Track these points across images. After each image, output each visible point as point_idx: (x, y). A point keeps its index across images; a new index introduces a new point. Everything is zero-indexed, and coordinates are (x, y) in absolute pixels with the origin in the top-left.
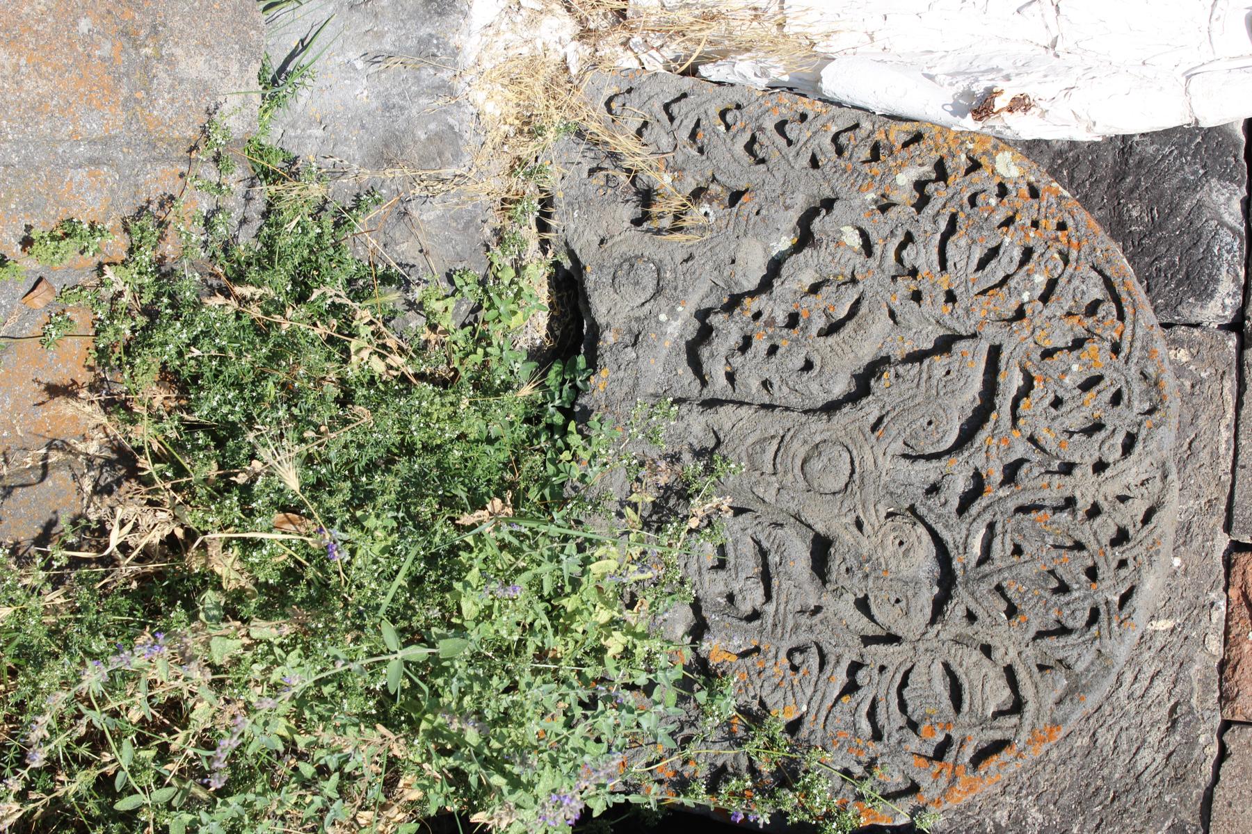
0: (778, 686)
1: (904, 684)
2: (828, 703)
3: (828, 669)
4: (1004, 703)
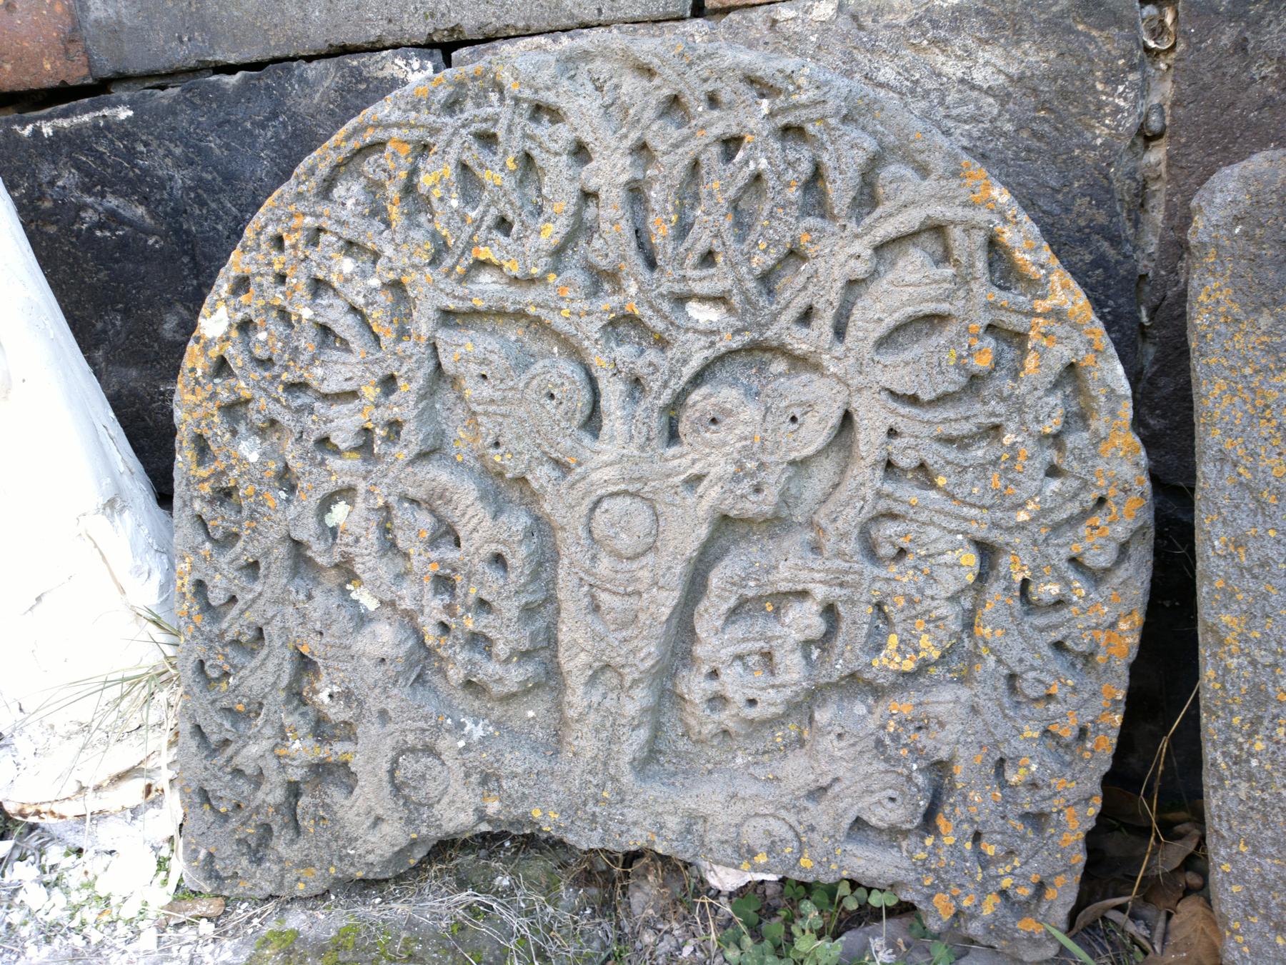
1: (913, 400)
2: (951, 506)
3: (898, 508)
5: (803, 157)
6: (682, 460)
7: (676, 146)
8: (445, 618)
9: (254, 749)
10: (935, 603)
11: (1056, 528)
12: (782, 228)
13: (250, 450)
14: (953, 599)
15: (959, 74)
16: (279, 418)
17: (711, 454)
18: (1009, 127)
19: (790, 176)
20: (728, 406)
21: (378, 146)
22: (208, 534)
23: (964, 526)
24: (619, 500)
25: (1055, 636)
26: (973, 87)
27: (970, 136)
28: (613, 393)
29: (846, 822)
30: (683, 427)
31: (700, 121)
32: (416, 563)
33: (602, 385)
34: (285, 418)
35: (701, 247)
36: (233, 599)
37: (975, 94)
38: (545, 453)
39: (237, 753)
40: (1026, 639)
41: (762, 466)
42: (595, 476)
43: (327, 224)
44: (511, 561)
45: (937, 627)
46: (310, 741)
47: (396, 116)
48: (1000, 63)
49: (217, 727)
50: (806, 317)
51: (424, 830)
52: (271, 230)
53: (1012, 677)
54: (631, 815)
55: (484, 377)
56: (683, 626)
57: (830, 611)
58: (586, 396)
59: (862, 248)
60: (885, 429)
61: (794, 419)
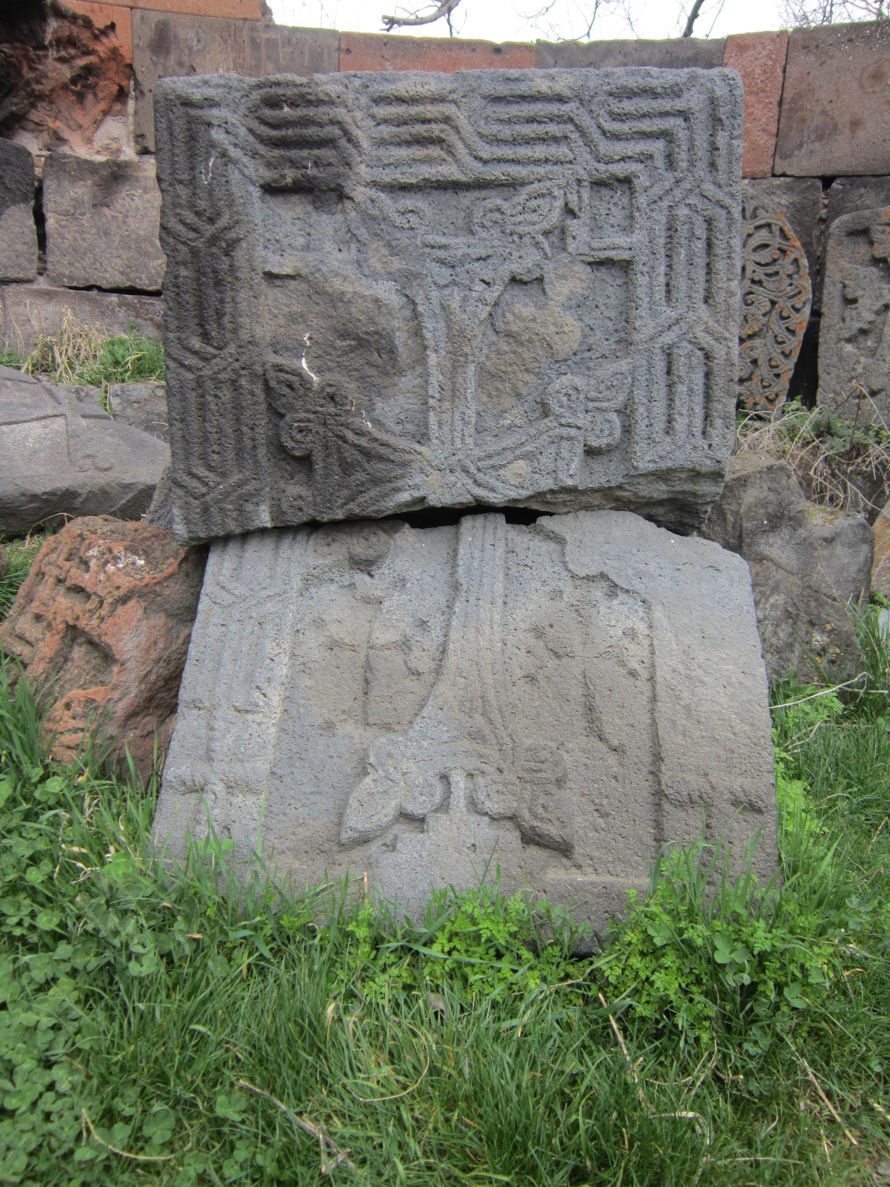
14: (764, 315)
53: (776, 336)
59: (752, 227)
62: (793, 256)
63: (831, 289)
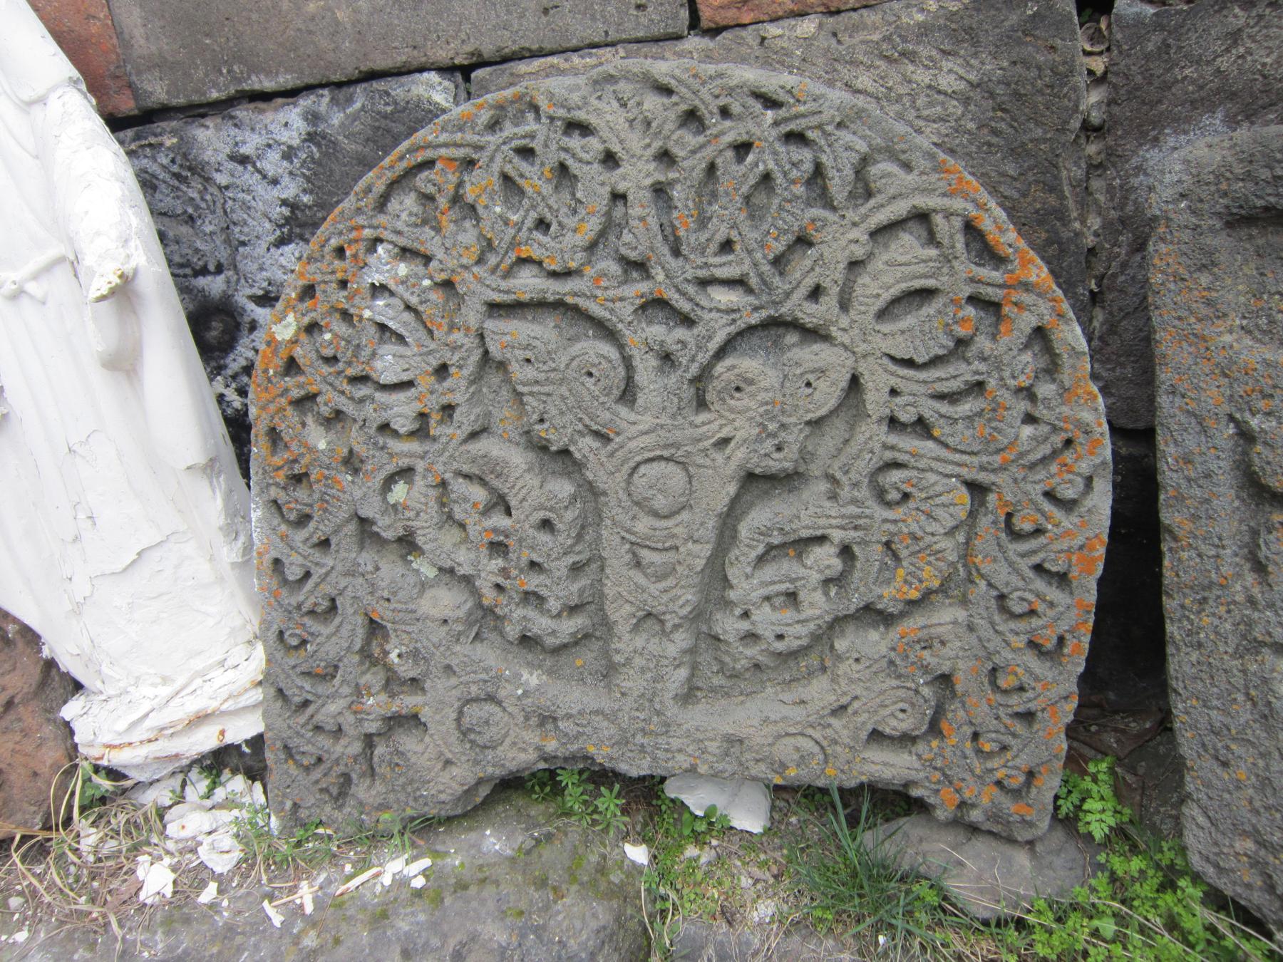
0: (929, 515)
1: (909, 363)
2: (944, 453)
3: (902, 458)
4: (918, 238)
5: (806, 155)
6: (710, 425)
7: (694, 152)
8: (500, 580)
9: (333, 708)
10: (935, 539)
11: (1032, 466)
12: (789, 218)
13: (320, 440)
14: (951, 533)
15: (927, 81)
16: (344, 409)
17: (737, 420)
18: (971, 126)
19: (795, 174)
20: (750, 375)
21: (429, 164)
22: (282, 516)
23: (957, 470)
24: (655, 464)
25: (1036, 559)
26: (939, 92)
27: (939, 133)
28: (646, 368)
29: (864, 735)
30: (710, 396)
31: (714, 131)
32: (473, 530)
33: (636, 362)
34: (349, 408)
35: (720, 237)
36: (307, 575)
37: (941, 97)
38: (586, 426)
39: (317, 711)
40: (1011, 564)
41: (783, 426)
42: (632, 445)
43: (386, 235)
44: (559, 526)
45: (937, 559)
46: (383, 697)
47: (444, 137)
48: (961, 71)
49: (300, 688)
50: (816, 293)
51: (490, 770)
52: (334, 242)
53: (1002, 597)
54: (675, 743)
55: (528, 361)
56: (716, 575)
57: (846, 551)
58: (621, 371)
59: (860, 234)
60: (887, 390)
61: (809, 384)
62: (1027, 321)
63: (1191, 442)
